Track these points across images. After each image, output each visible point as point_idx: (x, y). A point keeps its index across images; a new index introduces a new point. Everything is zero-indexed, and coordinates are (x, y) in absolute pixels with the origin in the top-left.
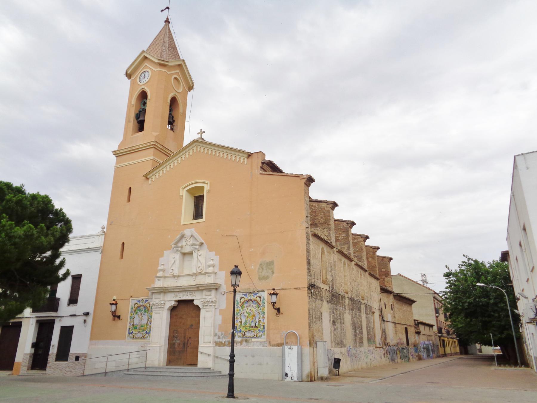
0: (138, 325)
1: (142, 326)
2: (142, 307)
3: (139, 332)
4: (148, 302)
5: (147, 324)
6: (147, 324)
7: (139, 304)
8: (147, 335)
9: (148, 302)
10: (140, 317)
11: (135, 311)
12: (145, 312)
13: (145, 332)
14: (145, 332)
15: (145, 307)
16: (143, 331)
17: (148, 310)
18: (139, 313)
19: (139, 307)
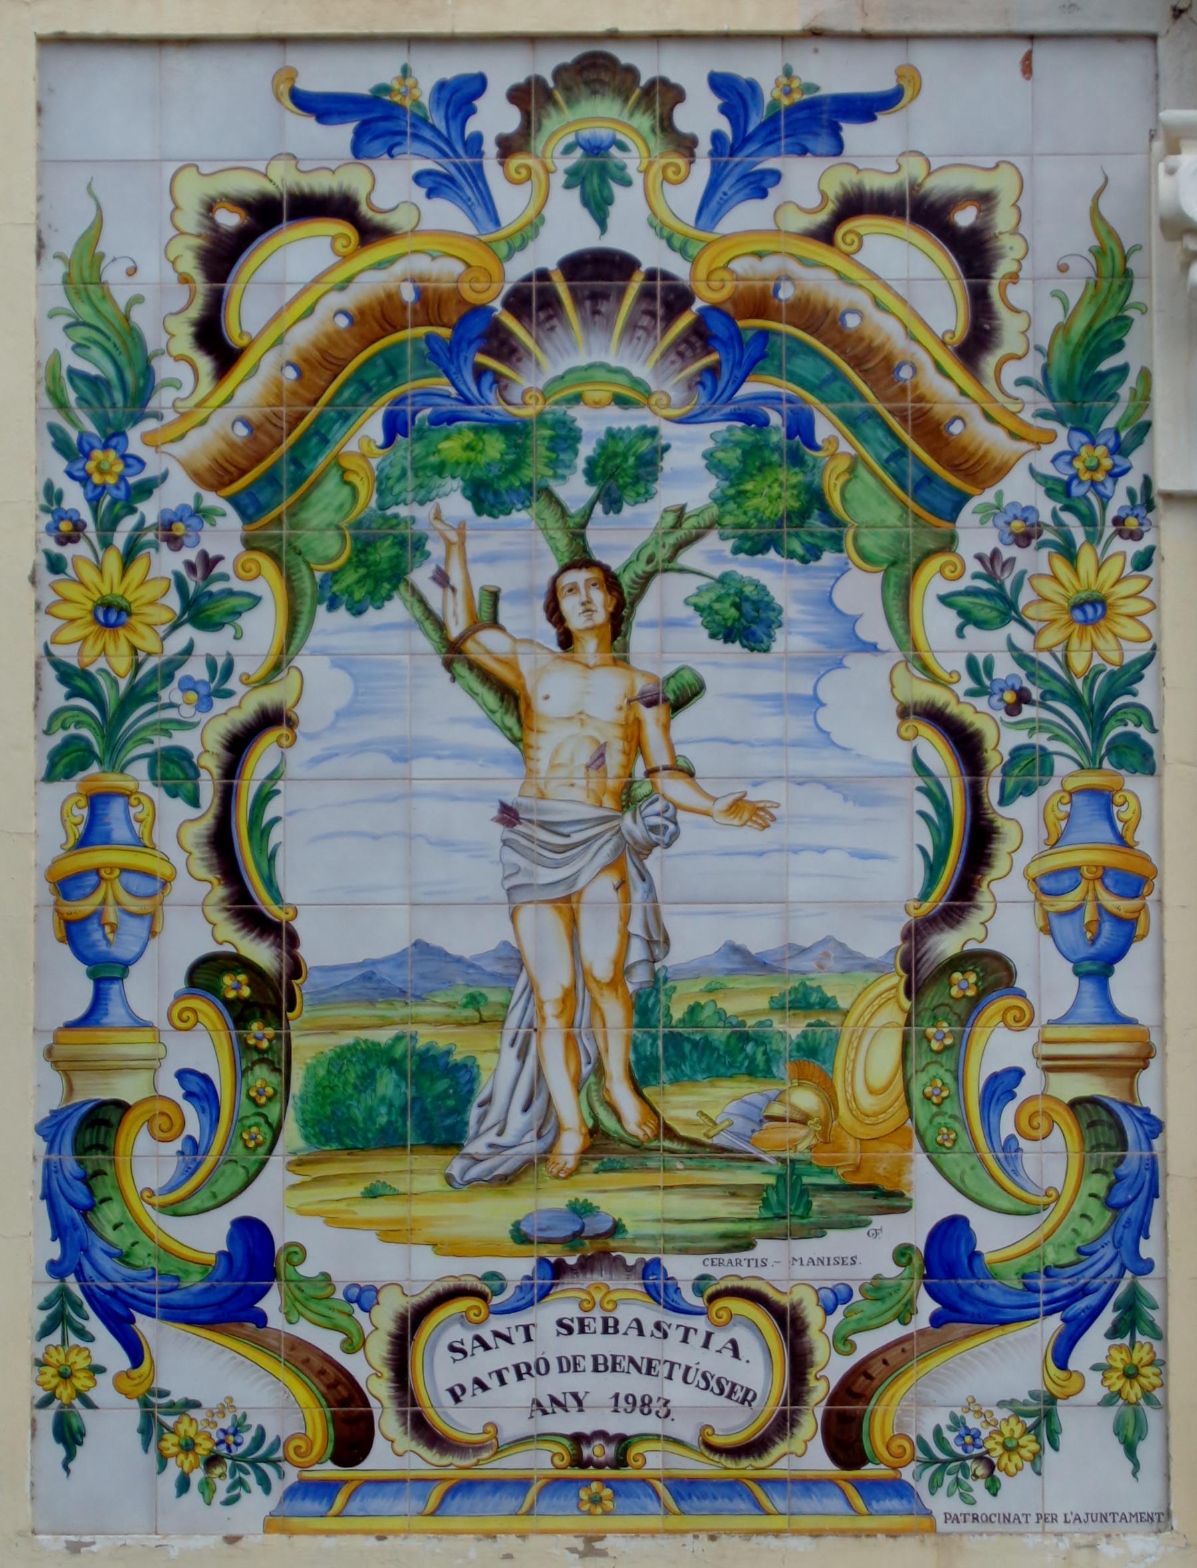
0: (489, 989)
1: (674, 1049)
2: (588, 369)
3: (581, 1252)
4: (875, 155)
5: (946, 982)
6: (946, 982)
7: (432, 243)
8: (1003, 1366)
9: (875, 155)
10: (578, 699)
11: (263, 476)
12: (808, 528)
13: (874, 1250)
14: (874, 1250)
15: (725, 339)
16: (793, 1203)
17: (941, 476)
18: (510, 556)
19: (475, 335)
